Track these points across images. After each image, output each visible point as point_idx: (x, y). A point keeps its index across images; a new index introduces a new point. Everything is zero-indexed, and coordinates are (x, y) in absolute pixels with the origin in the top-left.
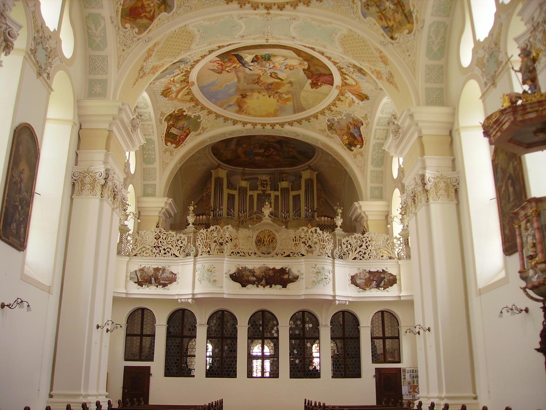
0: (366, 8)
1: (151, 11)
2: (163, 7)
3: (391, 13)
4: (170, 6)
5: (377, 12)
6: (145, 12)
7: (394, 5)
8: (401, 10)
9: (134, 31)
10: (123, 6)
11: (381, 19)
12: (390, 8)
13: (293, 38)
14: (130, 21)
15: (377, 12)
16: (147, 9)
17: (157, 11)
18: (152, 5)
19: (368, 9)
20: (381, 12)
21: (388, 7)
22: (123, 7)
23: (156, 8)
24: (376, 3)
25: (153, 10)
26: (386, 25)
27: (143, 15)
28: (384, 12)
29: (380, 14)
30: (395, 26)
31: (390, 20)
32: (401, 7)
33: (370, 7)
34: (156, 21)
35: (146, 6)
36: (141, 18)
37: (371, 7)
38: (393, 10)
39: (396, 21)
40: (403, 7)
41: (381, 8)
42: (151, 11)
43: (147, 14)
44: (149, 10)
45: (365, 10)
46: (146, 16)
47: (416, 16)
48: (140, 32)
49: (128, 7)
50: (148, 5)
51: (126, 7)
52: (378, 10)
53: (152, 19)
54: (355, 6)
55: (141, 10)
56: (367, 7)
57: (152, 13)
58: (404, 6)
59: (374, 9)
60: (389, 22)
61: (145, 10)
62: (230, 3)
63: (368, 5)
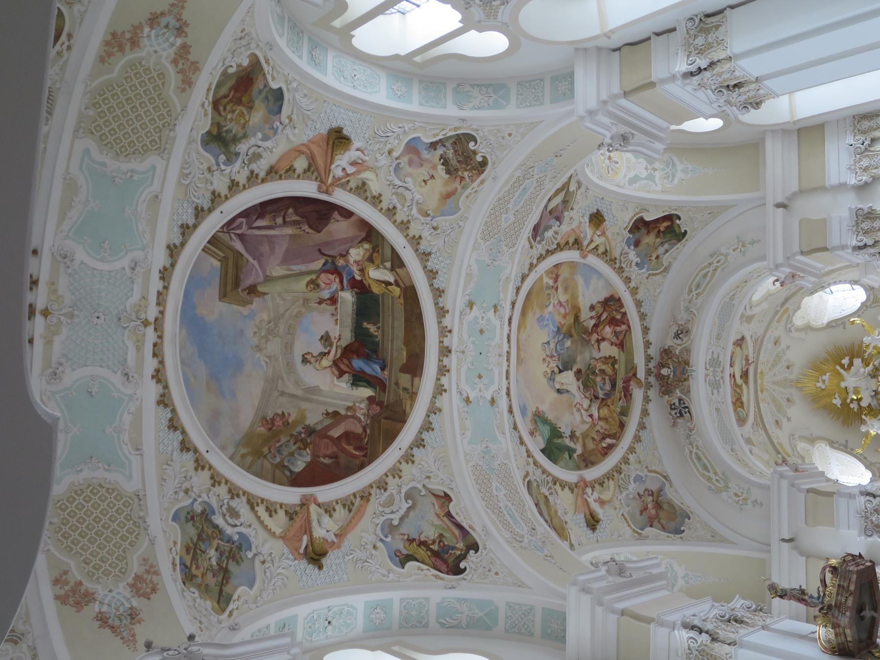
0: (186, 517)
1: (225, 109)
2: (215, 132)
3: (206, 564)
4: (207, 144)
5: (191, 539)
6: (230, 100)
7: (218, 564)
8: (220, 579)
9: (234, 65)
10: (264, 74)
11: (188, 550)
12: (210, 558)
13: (55, 375)
14: (244, 71)
15: (191, 539)
16: (231, 104)
17: (218, 118)
18: (229, 117)
19: (187, 521)
20: (195, 545)
21: (208, 556)
22: (262, 73)
23: (221, 120)
24: (202, 531)
25: (222, 113)
26: (188, 564)
27: (232, 94)
28: (199, 552)
29: (191, 545)
30: (199, 580)
31: (197, 568)
32: (223, 579)
33: (191, 522)
34: (209, 109)
35: (235, 107)
36: (230, 90)
37: (194, 525)
38: (211, 566)
39: (205, 578)
40: (224, 581)
41: (200, 543)
42: (225, 109)
43: (226, 100)
44: (228, 108)
45: (183, 515)
46: (225, 97)
47: (233, 609)
48: (224, 74)
49: (257, 79)
50: (234, 111)
51: (260, 78)
52: (195, 539)
53: (216, 104)
54: (182, 494)
55: (238, 95)
56: (189, 517)
57: (221, 108)
58: (227, 582)
59: (193, 532)
60: (194, 567)
61: (233, 101)
62: (168, 252)
63: (192, 518)
